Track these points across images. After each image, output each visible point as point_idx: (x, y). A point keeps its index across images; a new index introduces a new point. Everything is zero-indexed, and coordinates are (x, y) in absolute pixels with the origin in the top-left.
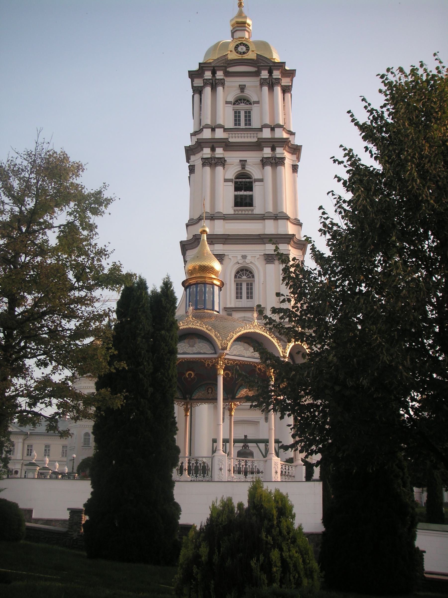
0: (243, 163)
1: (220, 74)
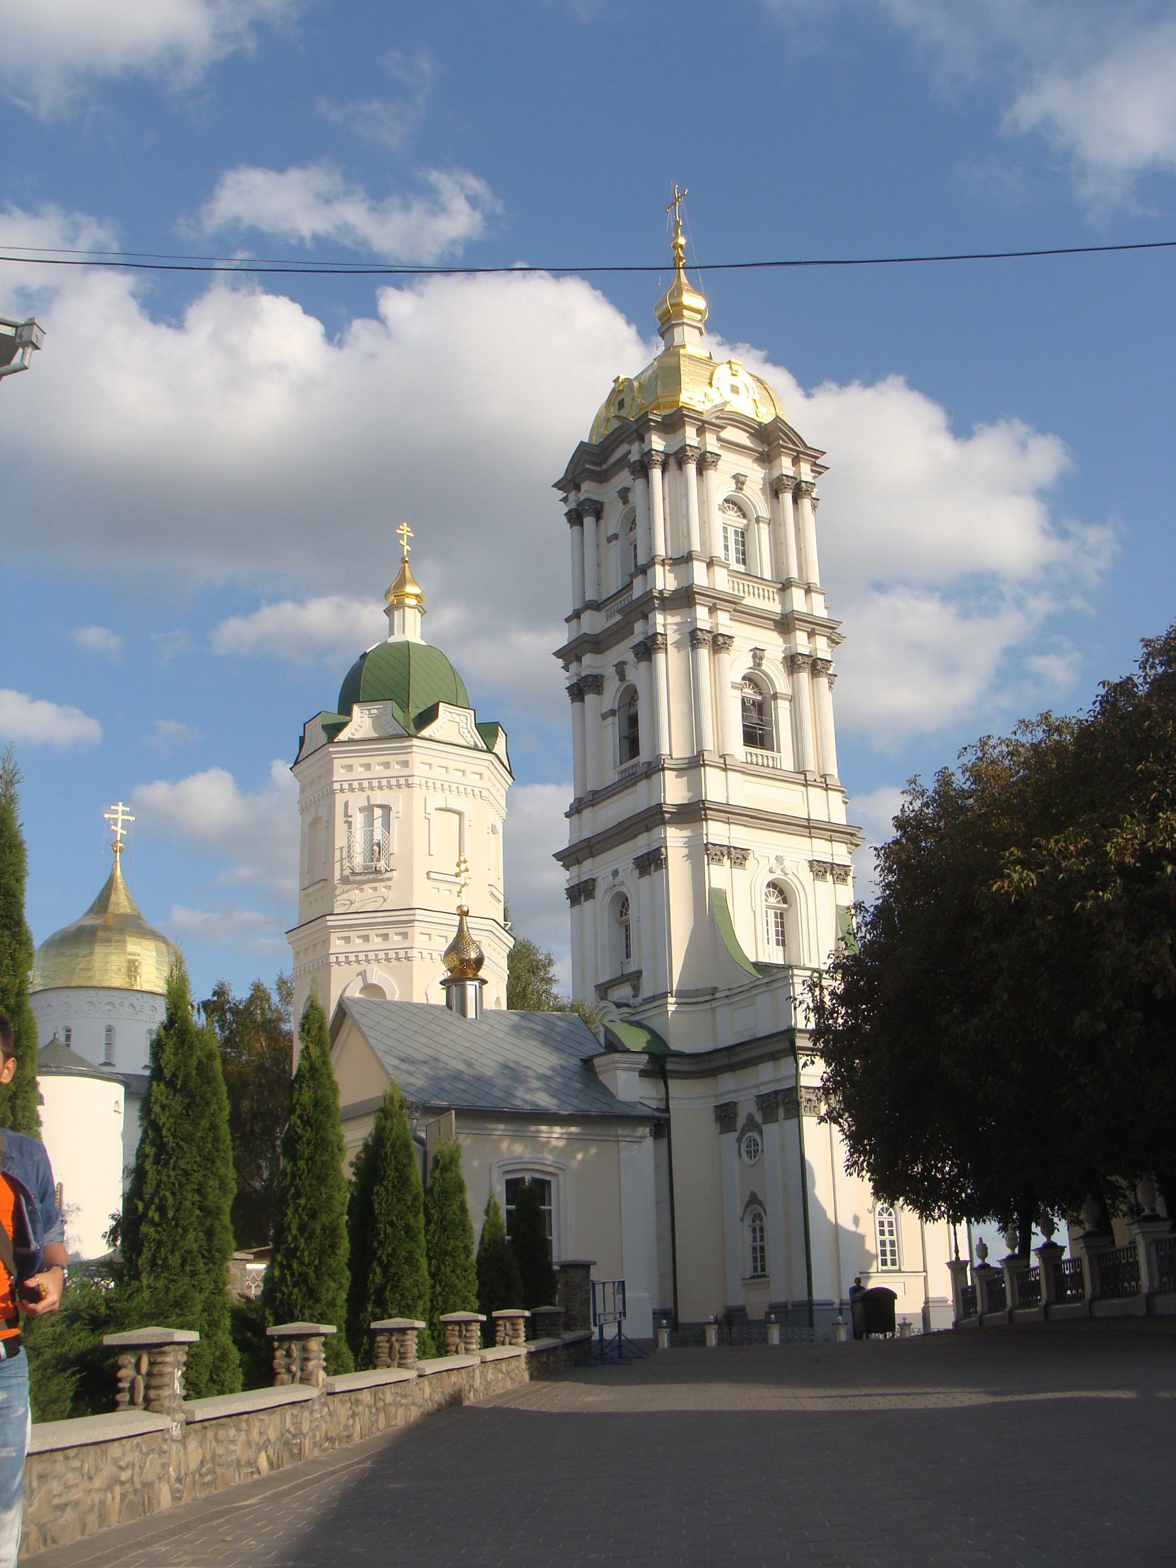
0: (758, 655)
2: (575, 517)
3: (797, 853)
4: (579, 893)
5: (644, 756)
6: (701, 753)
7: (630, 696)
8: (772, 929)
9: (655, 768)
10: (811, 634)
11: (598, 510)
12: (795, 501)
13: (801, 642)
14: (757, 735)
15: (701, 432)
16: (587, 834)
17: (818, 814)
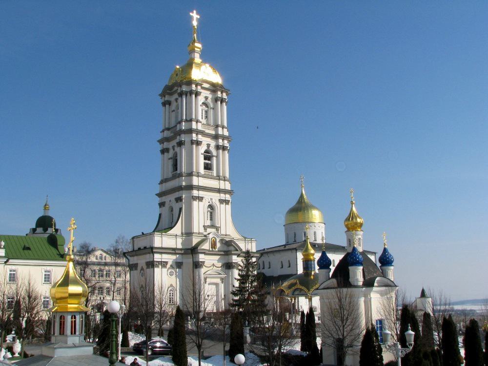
0: (208, 145)
1: (199, 87)
2: (164, 104)
3: (216, 197)
4: (162, 205)
5: (178, 172)
6: (192, 172)
7: (175, 155)
8: (209, 216)
9: (180, 175)
10: (223, 140)
11: (169, 103)
12: (221, 103)
13: (220, 142)
14: (208, 167)
15: (196, 86)
16: (164, 190)
17: (222, 187)
